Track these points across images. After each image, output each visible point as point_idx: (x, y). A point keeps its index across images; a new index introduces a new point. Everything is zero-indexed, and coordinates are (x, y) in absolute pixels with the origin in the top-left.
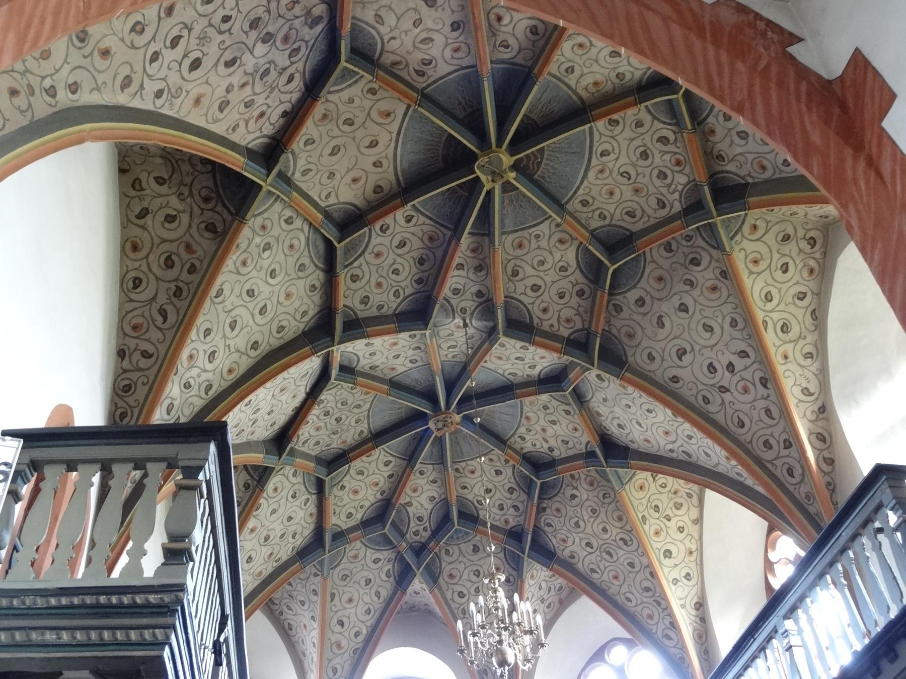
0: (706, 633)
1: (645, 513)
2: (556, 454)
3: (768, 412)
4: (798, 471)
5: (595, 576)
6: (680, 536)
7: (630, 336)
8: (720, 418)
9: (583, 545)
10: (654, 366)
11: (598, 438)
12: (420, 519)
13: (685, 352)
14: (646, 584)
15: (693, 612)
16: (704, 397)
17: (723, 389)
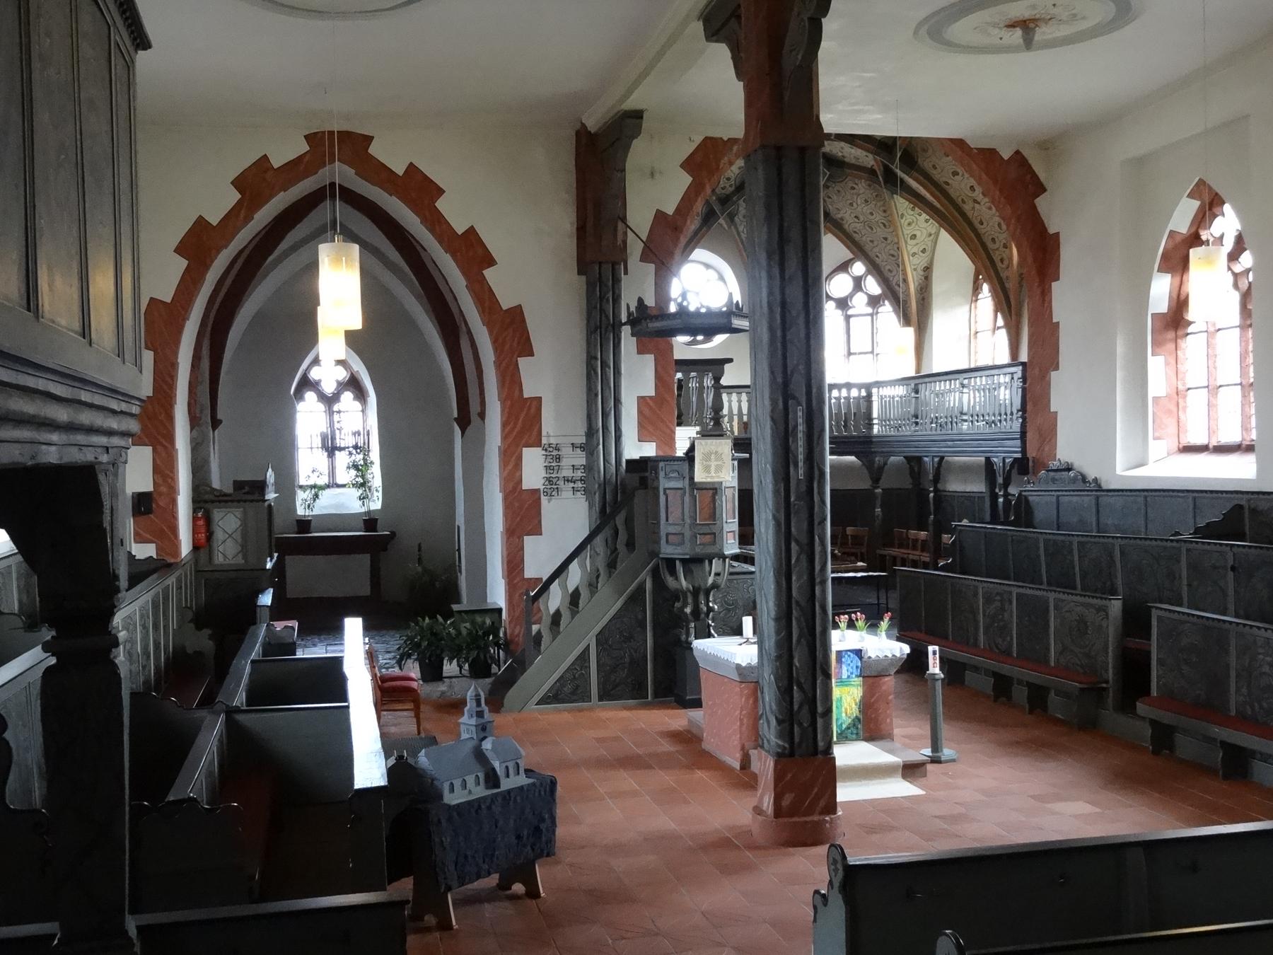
0: (927, 285)
1: (905, 212)
2: (846, 159)
3: (999, 225)
4: (1006, 263)
5: (855, 235)
6: (925, 225)
7: (925, 150)
8: (970, 214)
9: (853, 216)
10: (934, 172)
11: (882, 168)
12: (728, 179)
13: (958, 174)
14: (892, 252)
15: (922, 273)
16: (962, 200)
17: (975, 201)
